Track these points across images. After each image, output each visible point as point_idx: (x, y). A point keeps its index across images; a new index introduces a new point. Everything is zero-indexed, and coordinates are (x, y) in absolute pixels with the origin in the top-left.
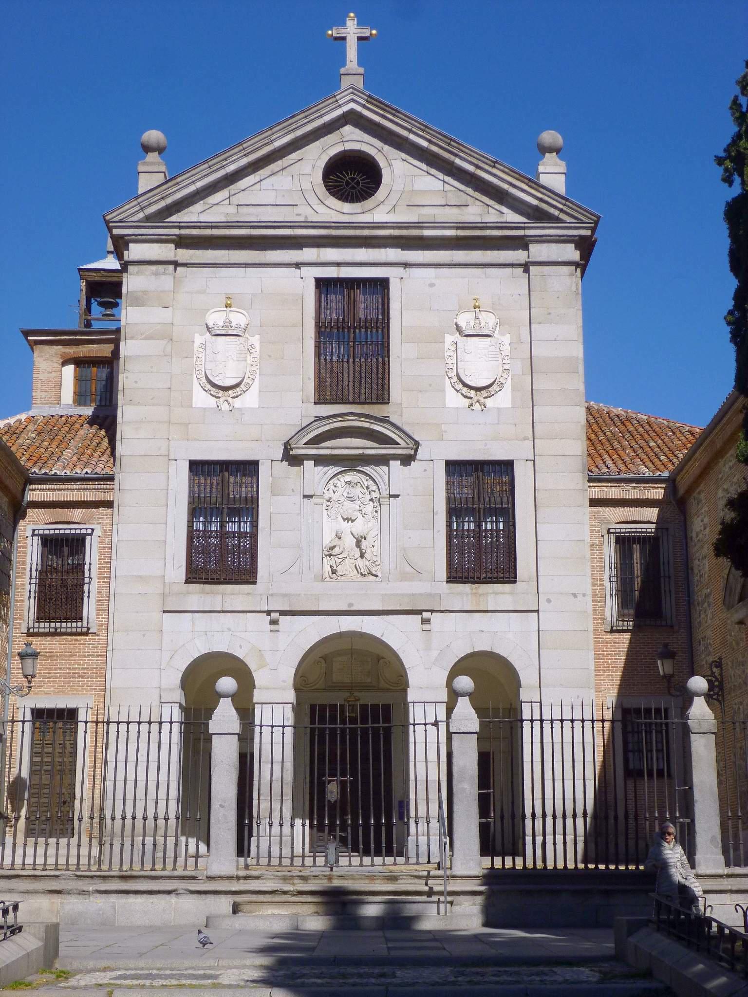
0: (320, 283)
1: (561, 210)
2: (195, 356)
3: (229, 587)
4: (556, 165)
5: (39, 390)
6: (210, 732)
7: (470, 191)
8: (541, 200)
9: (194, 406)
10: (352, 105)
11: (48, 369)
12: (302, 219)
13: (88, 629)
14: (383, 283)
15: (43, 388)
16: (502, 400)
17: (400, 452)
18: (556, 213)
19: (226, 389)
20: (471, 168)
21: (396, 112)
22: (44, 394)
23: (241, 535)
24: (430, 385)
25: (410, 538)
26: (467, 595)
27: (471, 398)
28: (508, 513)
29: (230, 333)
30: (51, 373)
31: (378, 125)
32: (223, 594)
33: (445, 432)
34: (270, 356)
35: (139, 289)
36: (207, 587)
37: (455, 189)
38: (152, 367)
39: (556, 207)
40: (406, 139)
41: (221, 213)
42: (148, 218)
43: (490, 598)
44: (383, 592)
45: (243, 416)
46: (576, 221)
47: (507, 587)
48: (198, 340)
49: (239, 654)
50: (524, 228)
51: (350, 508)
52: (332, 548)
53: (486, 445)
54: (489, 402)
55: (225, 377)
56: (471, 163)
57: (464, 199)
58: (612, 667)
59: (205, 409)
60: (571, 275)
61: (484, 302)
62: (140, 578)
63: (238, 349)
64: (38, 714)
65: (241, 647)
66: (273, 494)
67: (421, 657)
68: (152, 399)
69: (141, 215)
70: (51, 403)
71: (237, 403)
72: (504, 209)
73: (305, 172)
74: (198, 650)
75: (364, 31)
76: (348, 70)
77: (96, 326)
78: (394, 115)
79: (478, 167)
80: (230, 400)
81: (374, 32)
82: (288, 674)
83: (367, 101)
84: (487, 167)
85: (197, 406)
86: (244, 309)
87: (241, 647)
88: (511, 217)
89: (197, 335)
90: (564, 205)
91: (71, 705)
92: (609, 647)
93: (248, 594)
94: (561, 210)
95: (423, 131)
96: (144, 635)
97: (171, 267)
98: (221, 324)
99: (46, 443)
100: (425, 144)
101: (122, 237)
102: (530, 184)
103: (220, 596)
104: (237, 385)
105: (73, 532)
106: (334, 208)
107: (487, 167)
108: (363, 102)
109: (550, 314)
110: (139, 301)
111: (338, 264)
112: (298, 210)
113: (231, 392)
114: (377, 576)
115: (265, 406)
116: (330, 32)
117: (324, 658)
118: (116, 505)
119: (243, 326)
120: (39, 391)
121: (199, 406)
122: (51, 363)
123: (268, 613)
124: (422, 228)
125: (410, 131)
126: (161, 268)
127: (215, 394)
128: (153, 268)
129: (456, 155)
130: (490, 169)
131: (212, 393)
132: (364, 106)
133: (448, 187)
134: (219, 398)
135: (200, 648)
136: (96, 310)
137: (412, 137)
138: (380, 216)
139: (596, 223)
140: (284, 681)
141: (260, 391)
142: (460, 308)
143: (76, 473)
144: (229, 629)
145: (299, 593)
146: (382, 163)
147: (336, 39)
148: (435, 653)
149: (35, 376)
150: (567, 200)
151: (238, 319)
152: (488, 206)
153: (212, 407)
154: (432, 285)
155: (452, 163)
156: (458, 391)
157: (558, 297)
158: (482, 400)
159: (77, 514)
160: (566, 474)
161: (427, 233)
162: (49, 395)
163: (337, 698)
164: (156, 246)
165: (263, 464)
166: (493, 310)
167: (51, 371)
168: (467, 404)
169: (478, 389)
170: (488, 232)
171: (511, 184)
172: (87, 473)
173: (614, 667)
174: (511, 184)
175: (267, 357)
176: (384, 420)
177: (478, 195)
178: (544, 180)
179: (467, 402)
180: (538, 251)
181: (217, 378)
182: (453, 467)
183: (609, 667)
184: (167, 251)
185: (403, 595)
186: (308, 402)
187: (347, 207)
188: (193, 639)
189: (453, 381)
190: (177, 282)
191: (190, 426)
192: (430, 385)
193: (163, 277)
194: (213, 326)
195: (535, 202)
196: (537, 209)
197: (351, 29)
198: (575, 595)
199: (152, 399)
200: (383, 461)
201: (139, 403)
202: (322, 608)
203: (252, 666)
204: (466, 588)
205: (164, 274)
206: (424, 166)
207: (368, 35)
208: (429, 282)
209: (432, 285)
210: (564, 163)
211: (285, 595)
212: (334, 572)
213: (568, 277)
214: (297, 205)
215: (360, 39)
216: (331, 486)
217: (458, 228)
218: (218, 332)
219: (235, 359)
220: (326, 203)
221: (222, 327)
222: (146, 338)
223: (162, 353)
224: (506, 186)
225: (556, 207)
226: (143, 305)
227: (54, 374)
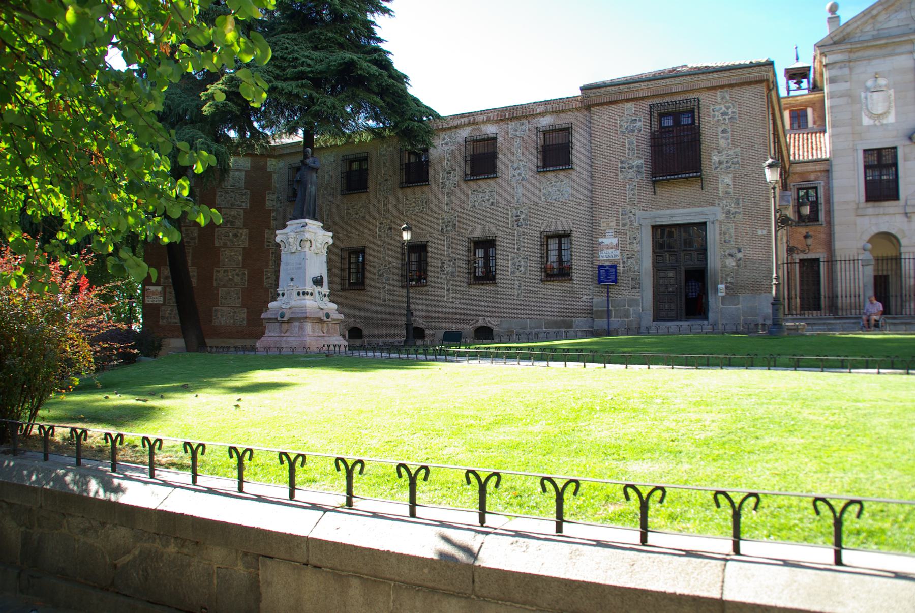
23: (888, 181)
36: (877, 204)
48: (863, 95)
49: (893, 232)
62: (845, 203)
64: (801, 260)
66: (905, 160)
69: (832, 42)
77: (792, 93)
91: (818, 257)
104: (885, 113)
126: (843, 64)
128: (838, 65)
135: (875, 230)
164: (840, 55)
190: (851, 69)
193: (844, 69)
203: (899, 236)
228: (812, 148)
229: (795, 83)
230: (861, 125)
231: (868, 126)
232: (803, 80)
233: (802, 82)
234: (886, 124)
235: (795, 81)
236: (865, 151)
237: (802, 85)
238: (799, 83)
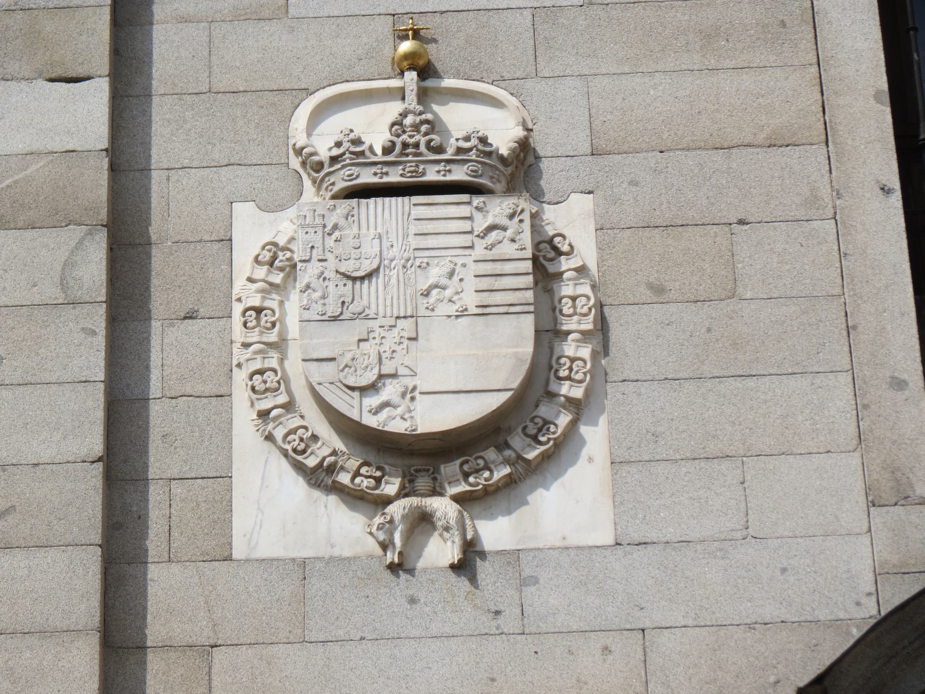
2: (238, 309)
9: (236, 555)
29: (432, 175)
34: (658, 290)
45: (529, 591)
55: (409, 393)
59: (303, 563)
63: (479, 251)
85: (261, 553)
89: (244, 213)
113: (451, 469)
115: (652, 536)
121: (264, 551)
127: (365, 483)
153: (347, 553)
175: (646, 294)
181: (372, 401)
191: (218, 655)
194: (336, 152)
218: (367, 177)
219: (471, 300)
221: (387, 151)
223: (51, 292)
230: (228, 558)
234: (512, 557)
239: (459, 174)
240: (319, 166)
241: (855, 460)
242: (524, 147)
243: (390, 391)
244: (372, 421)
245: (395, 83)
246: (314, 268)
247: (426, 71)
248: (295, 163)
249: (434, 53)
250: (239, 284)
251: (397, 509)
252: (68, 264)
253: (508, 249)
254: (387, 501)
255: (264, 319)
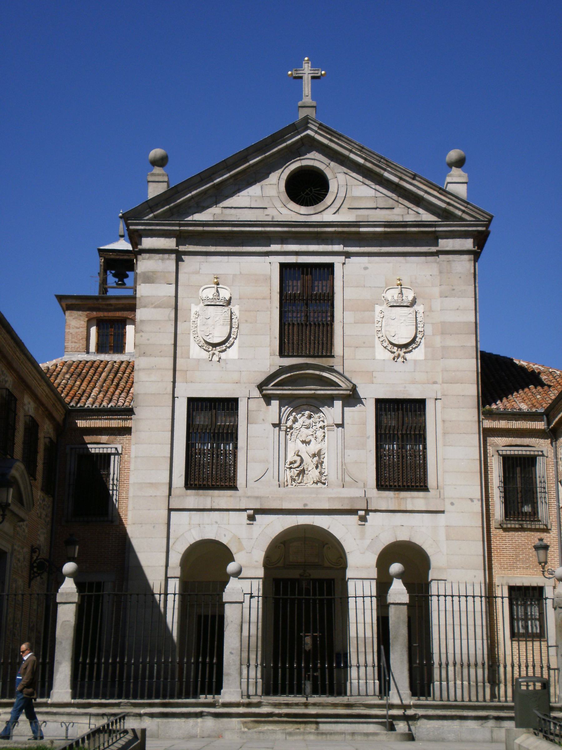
0: (283, 267)
1: (464, 212)
2: (191, 321)
3: (216, 492)
4: (460, 176)
5: (70, 342)
6: (224, 601)
7: (394, 196)
8: (449, 204)
9: (191, 357)
10: (309, 132)
11: (76, 326)
12: (269, 219)
13: (112, 522)
14: (331, 266)
15: (73, 340)
16: (418, 354)
17: (341, 392)
18: (459, 213)
19: (215, 345)
20: (396, 180)
21: (340, 136)
22: (73, 345)
24: (364, 343)
25: (349, 456)
26: (391, 498)
27: (394, 353)
28: (421, 437)
30: (79, 328)
31: (327, 146)
32: (212, 497)
33: (375, 377)
34: (246, 321)
35: (150, 270)
37: (384, 195)
38: (160, 329)
39: (459, 209)
40: (348, 158)
41: (211, 213)
42: (155, 217)
43: (409, 501)
44: (330, 496)
46: (474, 219)
47: (421, 494)
48: (194, 309)
49: (224, 541)
50: (435, 226)
51: (305, 433)
52: (291, 463)
53: (405, 387)
54: (408, 356)
56: (396, 176)
57: (390, 203)
58: (500, 554)
60: (470, 260)
61: (406, 282)
63: (223, 316)
65: (225, 535)
67: (358, 545)
68: (160, 352)
70: (79, 351)
71: (223, 355)
72: (421, 211)
73: (272, 183)
74: (194, 538)
75: (316, 72)
76: (304, 103)
77: (111, 293)
78: (339, 139)
79: (401, 178)
80: (217, 353)
81: (323, 72)
82: (259, 556)
83: (319, 128)
84: (407, 179)
86: (228, 286)
87: (225, 535)
88: (426, 216)
90: (466, 207)
92: (498, 539)
93: (231, 496)
94: (464, 212)
95: (361, 151)
96: (154, 527)
97: (174, 256)
98: (211, 297)
99: (78, 383)
100: (361, 161)
101: (137, 230)
102: (441, 191)
103: (210, 498)
105: (101, 451)
106: (293, 210)
107: (407, 179)
108: (316, 129)
109: (454, 290)
110: (149, 279)
111: (297, 253)
112: (267, 212)
114: (324, 484)
116: (290, 73)
117: (284, 543)
118: (133, 430)
119: (227, 298)
120: (70, 342)
121: (195, 357)
122: (79, 321)
123: (245, 510)
124: (359, 226)
125: (351, 151)
126: (166, 256)
127: (207, 349)
129: (385, 170)
130: (410, 180)
131: (204, 348)
132: (316, 132)
133: (379, 194)
134: (210, 351)
135: (195, 536)
136: (111, 280)
137: (352, 156)
138: (328, 217)
139: (490, 221)
140: (257, 562)
141: (239, 347)
142: (387, 285)
143: (104, 406)
144: (216, 522)
145: (267, 496)
146: (329, 174)
147: (295, 78)
148: (368, 542)
149: (67, 330)
150: (468, 203)
151: (225, 294)
152: (409, 208)
154: (366, 268)
155: (381, 176)
156: (385, 347)
157: (460, 277)
158: (402, 353)
159: (104, 438)
160: (465, 409)
161: (362, 229)
162: (77, 345)
163: (294, 574)
165: (241, 401)
166: (411, 286)
167: (78, 326)
168: (392, 356)
169: (400, 347)
170: (408, 229)
171: (426, 192)
172: (112, 406)
173: (502, 554)
174: (426, 192)
176: (331, 370)
177: (401, 200)
178: (451, 188)
179: (392, 356)
180: (445, 244)
182: (380, 403)
183: (498, 554)
184: (170, 243)
185: (344, 498)
186: (274, 355)
187: (303, 210)
188: (190, 530)
189: (381, 339)
191: (188, 372)
192: (364, 343)
195: (443, 205)
196: (445, 210)
197: (307, 70)
198: (472, 500)
199: (160, 352)
200: (329, 401)
201: (151, 355)
202: (285, 507)
204: (390, 494)
205: (168, 259)
206: (360, 178)
207: (319, 75)
208: (364, 266)
209: (366, 268)
210: (466, 175)
211: (257, 498)
212: (293, 480)
213: (468, 262)
214: (266, 208)
215: (313, 78)
216: (291, 418)
217: (385, 226)
219: (222, 323)
220: (288, 206)
222: (155, 307)
224: (421, 193)
225: (459, 209)
226: (153, 283)
227: (81, 330)
228: (118, 385)
229: (115, 275)
231: (199, 360)
232: (128, 273)
233: (127, 276)
234: (225, 360)
235: (113, 272)
236: (191, 401)
237: (126, 280)
238: (121, 276)
239: (221, 304)
240: (203, 300)
241: (269, 348)
242: (231, 298)
243: (210, 336)
244: (208, 341)
245: (213, 286)
246: (202, 317)
247: (218, 284)
248: (200, 298)
249: (219, 280)
250: (192, 317)
251: (211, 353)
252: (169, 314)
253: (227, 315)
254: (210, 351)
255: (195, 323)
